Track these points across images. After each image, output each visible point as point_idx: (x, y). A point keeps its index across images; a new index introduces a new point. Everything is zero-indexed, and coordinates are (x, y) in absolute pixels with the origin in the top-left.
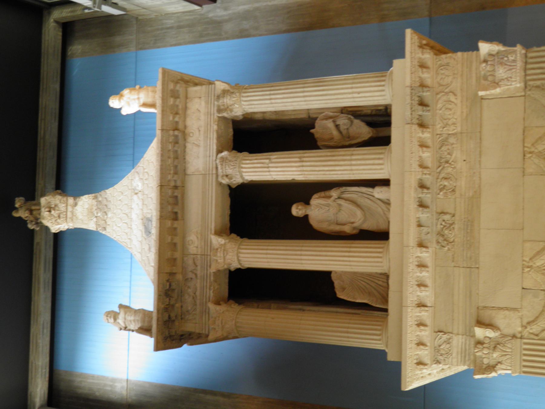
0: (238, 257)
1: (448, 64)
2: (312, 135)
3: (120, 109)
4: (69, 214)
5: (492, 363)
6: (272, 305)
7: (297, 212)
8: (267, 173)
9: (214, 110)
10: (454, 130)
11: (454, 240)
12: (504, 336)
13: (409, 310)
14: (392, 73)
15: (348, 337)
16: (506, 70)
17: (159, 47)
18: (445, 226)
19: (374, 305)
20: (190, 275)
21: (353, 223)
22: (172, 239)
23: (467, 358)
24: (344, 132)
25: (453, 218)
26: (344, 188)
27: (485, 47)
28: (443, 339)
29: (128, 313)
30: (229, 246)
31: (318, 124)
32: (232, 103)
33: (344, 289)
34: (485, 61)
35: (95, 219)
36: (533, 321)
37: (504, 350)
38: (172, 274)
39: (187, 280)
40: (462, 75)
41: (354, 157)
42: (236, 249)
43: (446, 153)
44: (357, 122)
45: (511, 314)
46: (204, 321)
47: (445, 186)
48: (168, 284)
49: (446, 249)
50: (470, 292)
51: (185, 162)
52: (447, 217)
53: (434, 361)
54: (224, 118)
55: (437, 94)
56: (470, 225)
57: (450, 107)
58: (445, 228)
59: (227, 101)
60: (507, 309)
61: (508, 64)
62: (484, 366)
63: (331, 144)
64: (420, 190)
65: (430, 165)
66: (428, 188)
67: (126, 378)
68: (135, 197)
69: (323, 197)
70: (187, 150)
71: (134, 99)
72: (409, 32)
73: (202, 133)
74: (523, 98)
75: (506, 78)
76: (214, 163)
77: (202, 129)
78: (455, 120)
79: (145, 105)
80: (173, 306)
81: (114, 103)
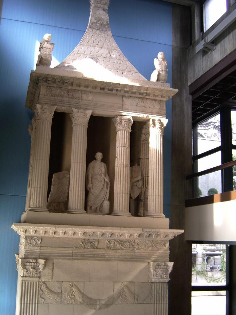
4: (99, 5)
8: (121, 146)
12: (40, 272)
13: (54, 228)
20: (71, 94)
26: (109, 183)
27: (171, 264)
28: (38, 241)
36: (47, 287)
38: (72, 84)
45: (51, 276)
47: (111, 243)
52: (96, 244)
55: (152, 240)
59: (158, 125)
60: (53, 274)
62: (25, 263)
66: (111, 236)
68: (107, 52)
71: (162, 68)
74: (147, 281)
79: (159, 74)
80: (55, 82)
81: (160, 55)
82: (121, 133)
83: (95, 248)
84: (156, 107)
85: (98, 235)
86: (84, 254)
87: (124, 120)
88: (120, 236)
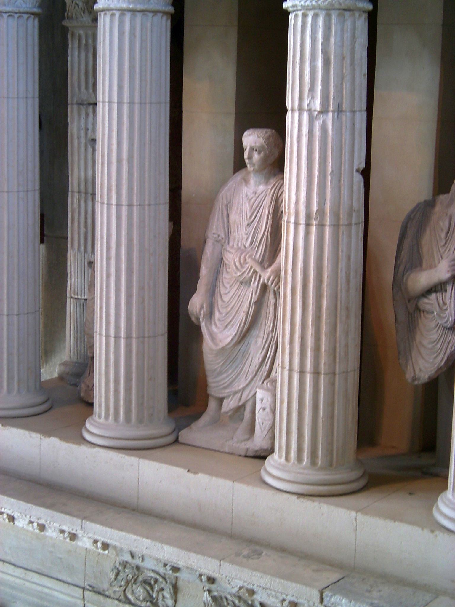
18: (152, 589)
58: (148, 588)
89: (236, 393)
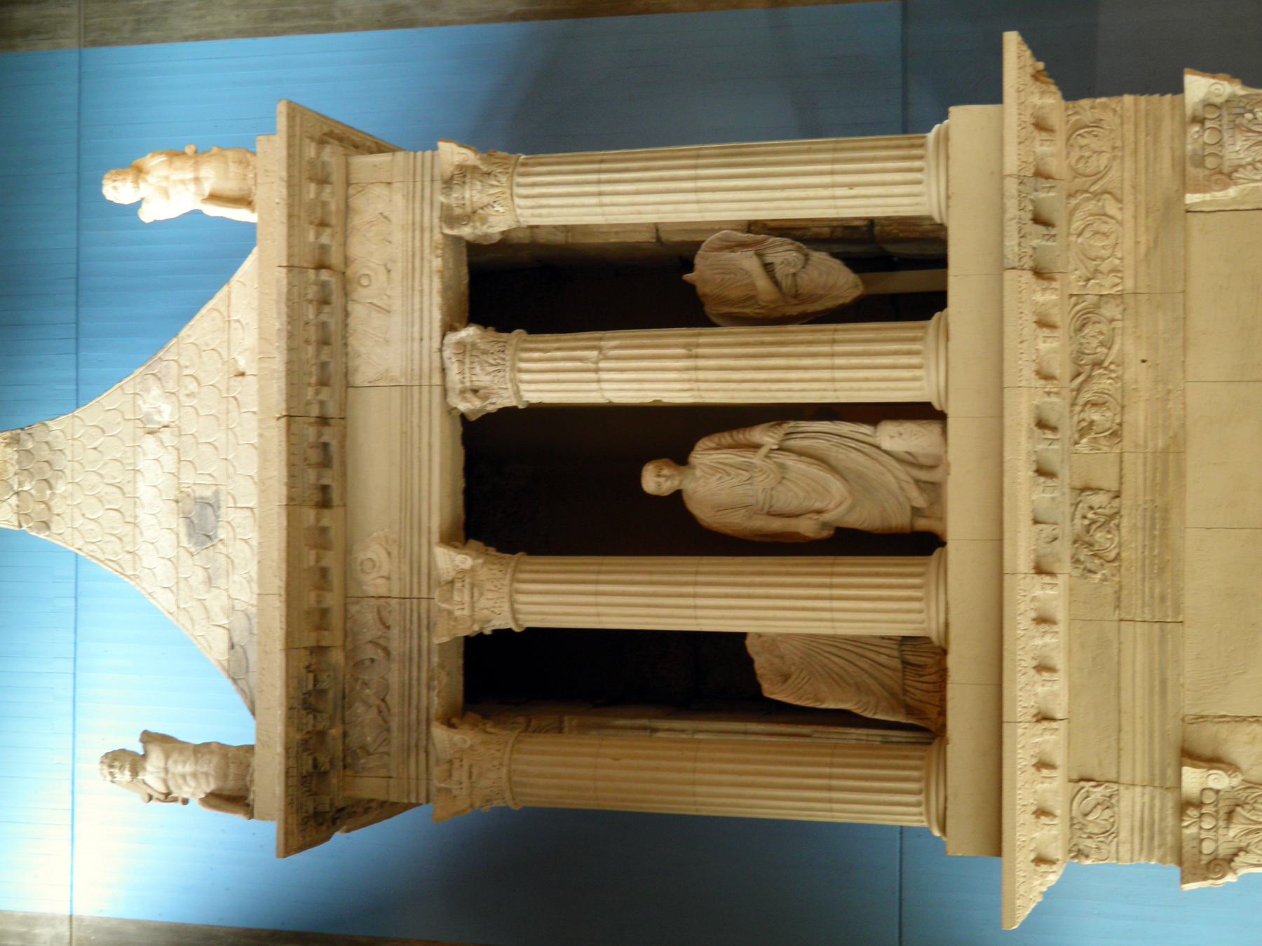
0: (512, 602)
1: (1097, 124)
2: (691, 287)
3: (138, 205)
5: (1224, 851)
6: (567, 720)
7: (659, 485)
8: (595, 386)
9: (432, 217)
10: (1117, 285)
11: (1118, 554)
13: (1020, 731)
14: (945, 139)
15: (830, 801)
16: (1249, 143)
17: (148, 41)
18: (1093, 522)
19: (869, 715)
20: (369, 652)
21: (819, 512)
22: (318, 559)
23: (1156, 842)
24: (786, 283)
25: (1116, 503)
26: (792, 423)
27: (1198, 86)
28: (1093, 796)
29: (175, 756)
30: (483, 574)
31: (702, 262)
32: (486, 200)
33: (786, 677)
34: (1199, 120)
35: (14, 500)
37: (1254, 818)
38: (319, 650)
39: (358, 664)
40: (1135, 151)
41: (839, 348)
42: (506, 582)
43: (1095, 343)
44: (820, 257)
46: (413, 774)
47: (1092, 423)
48: (311, 676)
49: (1099, 576)
50: (1163, 683)
51: (347, 354)
52: (1098, 500)
53: (1070, 851)
54: (457, 239)
55: (1070, 196)
56: (1161, 521)
57: (1104, 228)
58: (1094, 527)
59: (473, 194)
61: (1254, 128)
62: (1205, 860)
63: (749, 311)
64: (1037, 431)
65: (1057, 372)
66: (1054, 429)
67: (68, 913)
68: (149, 443)
69: (730, 447)
70: (352, 321)
71: (183, 182)
72: (1012, 41)
73: (397, 276)
75: (1252, 164)
76: (436, 357)
77: (398, 269)
78: (1117, 262)
79: (214, 198)
80: (321, 735)
81: (117, 190)
82: (533, 387)
83: (1120, 508)
84: (381, 207)
85: (1047, 496)
86: (1152, 564)
87: (467, 375)
88: (1048, 377)
89: (902, 489)
